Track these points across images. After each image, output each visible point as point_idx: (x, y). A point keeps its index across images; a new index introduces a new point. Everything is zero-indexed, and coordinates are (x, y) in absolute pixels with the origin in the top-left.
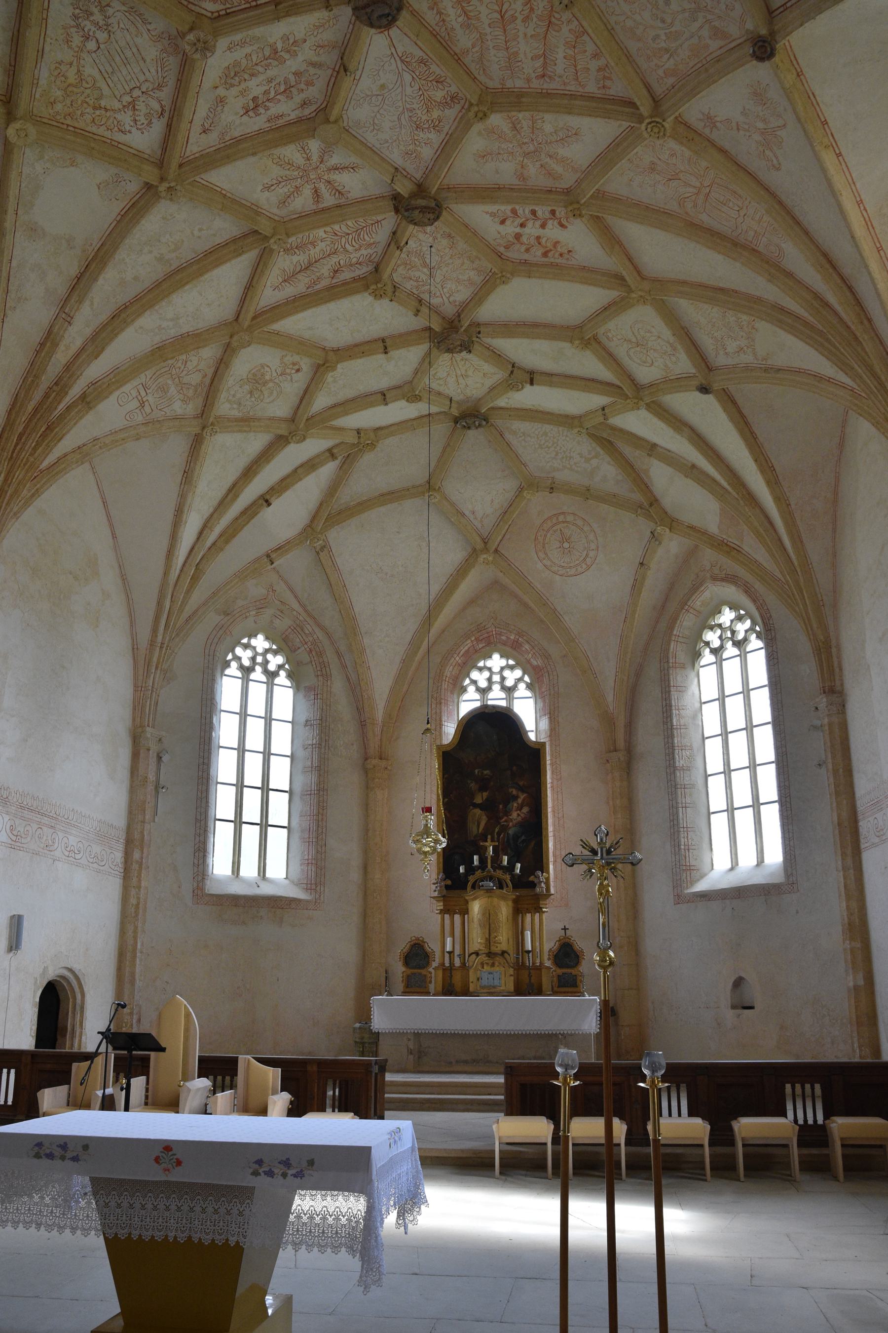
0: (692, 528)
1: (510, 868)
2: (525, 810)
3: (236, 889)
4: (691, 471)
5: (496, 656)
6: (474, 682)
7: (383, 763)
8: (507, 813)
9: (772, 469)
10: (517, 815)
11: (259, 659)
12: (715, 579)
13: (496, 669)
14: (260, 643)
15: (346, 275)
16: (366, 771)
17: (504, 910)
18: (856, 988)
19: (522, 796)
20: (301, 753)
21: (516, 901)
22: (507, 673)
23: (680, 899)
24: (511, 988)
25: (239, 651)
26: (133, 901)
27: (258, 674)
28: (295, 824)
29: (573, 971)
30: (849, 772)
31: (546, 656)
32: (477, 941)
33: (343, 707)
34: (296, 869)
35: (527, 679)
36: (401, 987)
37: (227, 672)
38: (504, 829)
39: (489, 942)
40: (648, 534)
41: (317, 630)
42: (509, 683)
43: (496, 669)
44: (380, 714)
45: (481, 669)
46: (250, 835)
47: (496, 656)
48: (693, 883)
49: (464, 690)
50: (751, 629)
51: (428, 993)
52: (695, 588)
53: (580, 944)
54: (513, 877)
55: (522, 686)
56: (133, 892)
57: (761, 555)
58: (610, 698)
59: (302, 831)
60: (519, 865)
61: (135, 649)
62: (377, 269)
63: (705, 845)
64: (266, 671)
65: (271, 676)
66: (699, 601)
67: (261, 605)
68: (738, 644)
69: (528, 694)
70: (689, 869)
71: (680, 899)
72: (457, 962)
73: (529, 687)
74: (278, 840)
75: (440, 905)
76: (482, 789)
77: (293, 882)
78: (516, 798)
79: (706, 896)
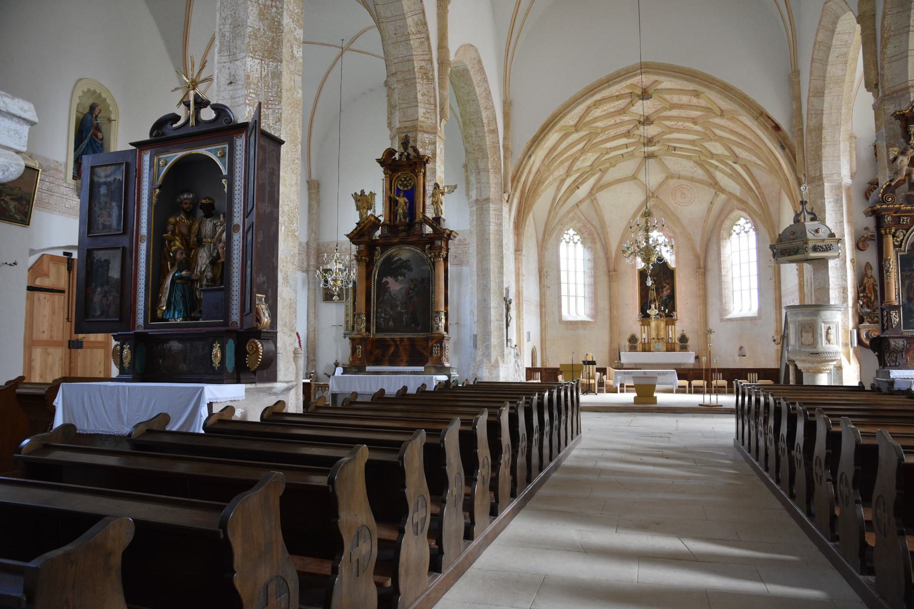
0: (730, 193)
1: (664, 311)
2: (669, 291)
3: (570, 319)
4: (730, 176)
7: (616, 273)
8: (662, 292)
9: (758, 183)
10: (666, 293)
11: (571, 238)
12: (738, 209)
14: (571, 232)
15: (619, 133)
16: (609, 276)
17: (663, 325)
18: (777, 350)
19: (668, 286)
20: (587, 271)
21: (666, 322)
24: (665, 349)
26: (544, 325)
27: (571, 243)
28: (587, 295)
29: (686, 344)
30: (780, 282)
31: (674, 233)
32: (653, 334)
33: (601, 254)
34: (588, 311)
36: (628, 349)
38: (661, 297)
39: (657, 335)
40: (714, 193)
44: (613, 255)
46: (572, 299)
48: (727, 315)
50: (751, 228)
51: (637, 351)
52: (731, 211)
53: (688, 335)
54: (665, 314)
56: (544, 322)
57: (754, 206)
58: (698, 249)
60: (667, 310)
61: (537, 242)
62: (629, 132)
63: (731, 302)
64: (574, 242)
66: (732, 216)
67: (572, 219)
70: (726, 310)
71: (722, 320)
72: (646, 342)
74: (581, 301)
75: (641, 323)
78: (665, 287)
79: (731, 320)
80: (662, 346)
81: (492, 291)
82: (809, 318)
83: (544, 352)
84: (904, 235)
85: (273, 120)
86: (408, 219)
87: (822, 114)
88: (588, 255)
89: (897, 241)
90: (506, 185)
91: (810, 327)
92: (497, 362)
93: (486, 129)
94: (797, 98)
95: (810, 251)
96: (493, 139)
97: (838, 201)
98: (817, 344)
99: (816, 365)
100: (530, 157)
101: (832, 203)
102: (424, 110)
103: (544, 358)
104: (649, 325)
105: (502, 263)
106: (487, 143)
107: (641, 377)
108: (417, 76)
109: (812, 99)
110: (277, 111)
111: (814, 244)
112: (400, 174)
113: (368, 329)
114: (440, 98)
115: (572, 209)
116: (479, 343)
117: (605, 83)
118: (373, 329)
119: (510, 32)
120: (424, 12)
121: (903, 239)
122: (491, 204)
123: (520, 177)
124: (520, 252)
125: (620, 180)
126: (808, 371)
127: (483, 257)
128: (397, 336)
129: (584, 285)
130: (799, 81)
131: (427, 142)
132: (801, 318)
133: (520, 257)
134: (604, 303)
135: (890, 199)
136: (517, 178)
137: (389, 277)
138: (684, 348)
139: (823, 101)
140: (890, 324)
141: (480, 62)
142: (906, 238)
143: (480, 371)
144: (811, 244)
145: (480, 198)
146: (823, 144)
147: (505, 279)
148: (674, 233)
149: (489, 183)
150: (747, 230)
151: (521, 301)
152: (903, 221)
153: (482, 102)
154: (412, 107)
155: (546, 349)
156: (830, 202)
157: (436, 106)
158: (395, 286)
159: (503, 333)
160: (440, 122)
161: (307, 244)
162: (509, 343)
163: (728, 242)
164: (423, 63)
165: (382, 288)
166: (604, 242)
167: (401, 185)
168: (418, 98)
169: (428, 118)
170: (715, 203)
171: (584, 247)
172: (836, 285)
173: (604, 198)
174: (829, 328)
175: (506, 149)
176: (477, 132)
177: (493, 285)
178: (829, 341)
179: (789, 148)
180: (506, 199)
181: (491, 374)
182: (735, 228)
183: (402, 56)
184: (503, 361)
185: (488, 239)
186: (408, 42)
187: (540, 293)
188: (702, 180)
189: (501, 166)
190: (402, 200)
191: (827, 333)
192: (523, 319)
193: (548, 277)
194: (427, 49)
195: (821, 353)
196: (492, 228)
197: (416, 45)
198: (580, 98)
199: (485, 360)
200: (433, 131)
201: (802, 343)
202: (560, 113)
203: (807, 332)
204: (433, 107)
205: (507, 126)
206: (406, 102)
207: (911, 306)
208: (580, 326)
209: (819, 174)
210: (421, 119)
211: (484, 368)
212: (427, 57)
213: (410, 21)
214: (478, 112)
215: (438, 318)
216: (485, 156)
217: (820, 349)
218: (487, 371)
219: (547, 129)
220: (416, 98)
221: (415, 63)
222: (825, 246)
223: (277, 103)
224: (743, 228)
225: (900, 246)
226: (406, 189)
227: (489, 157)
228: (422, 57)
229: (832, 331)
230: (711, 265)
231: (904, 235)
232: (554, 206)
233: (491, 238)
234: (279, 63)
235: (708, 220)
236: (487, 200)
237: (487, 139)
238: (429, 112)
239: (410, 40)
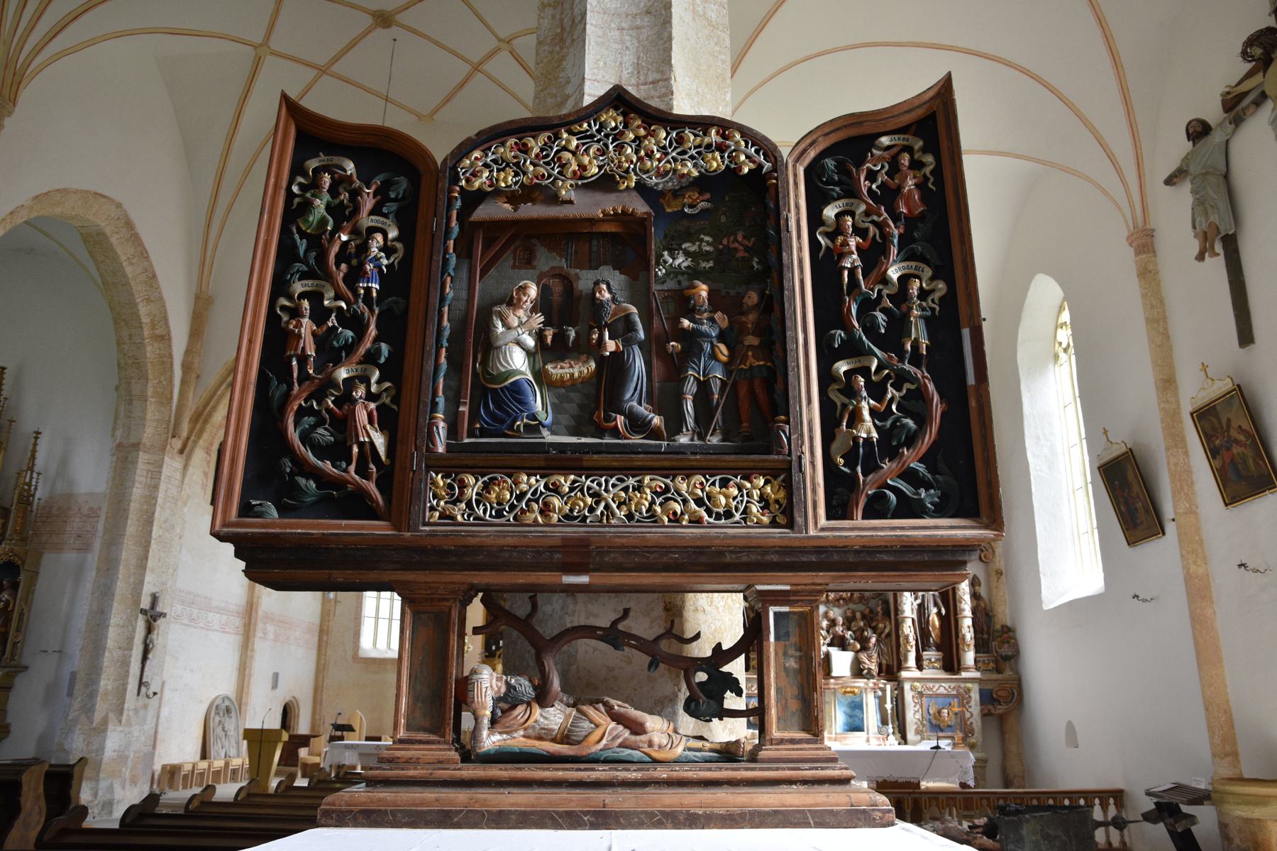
81: (117, 598)
83: (318, 707)
92: (105, 722)
93: (146, 333)
105: (148, 551)
116: (78, 687)
122: (141, 453)
123: (210, 415)
136: (203, 417)
141: (129, 225)
143: (69, 739)
147: (148, 578)
149: (143, 419)
151: (253, 621)
153: (139, 290)
175: (186, 367)
177: (122, 587)
184: (120, 721)
185: (126, 510)
192: (253, 651)
196: (138, 491)
199: (83, 718)
211: (77, 732)
216: (144, 377)
218: (81, 738)
227: (150, 377)
236: (136, 446)
237: (149, 348)
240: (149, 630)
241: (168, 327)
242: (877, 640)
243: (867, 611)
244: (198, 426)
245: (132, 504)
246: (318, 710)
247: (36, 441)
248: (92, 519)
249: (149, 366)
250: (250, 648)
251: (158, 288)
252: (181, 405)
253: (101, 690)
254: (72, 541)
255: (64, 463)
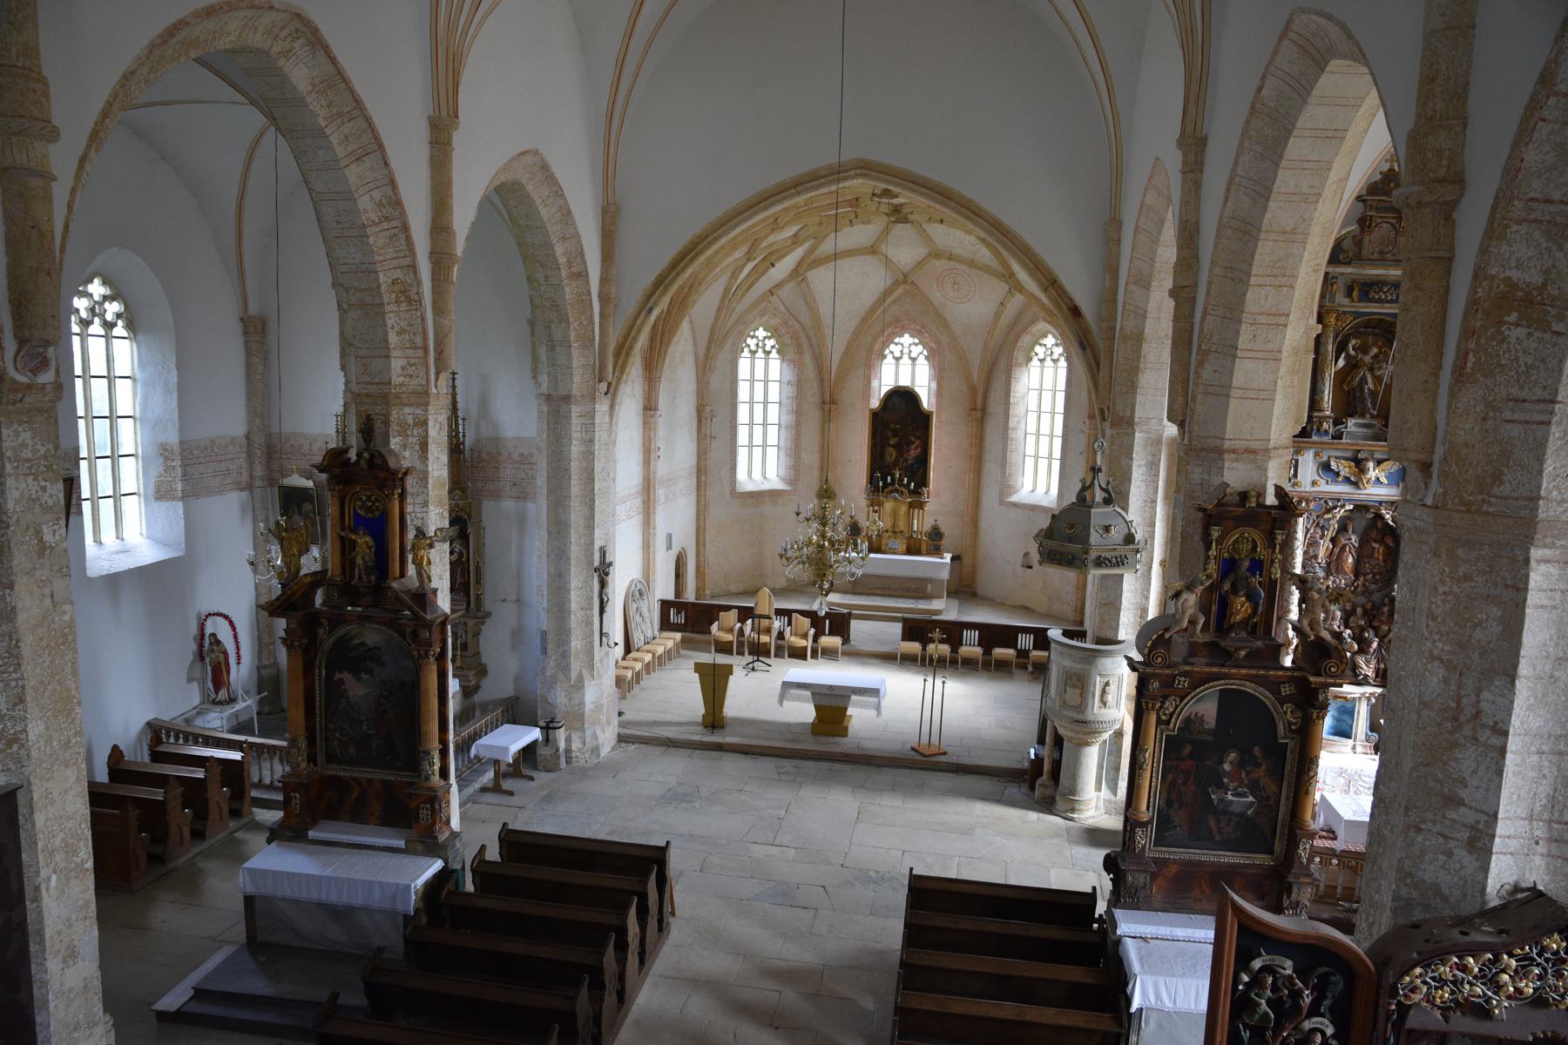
1: (909, 484)
2: (919, 450)
3: (750, 487)
5: (907, 336)
6: (892, 353)
8: (908, 451)
10: (914, 452)
12: (1045, 320)
13: (906, 345)
14: (761, 333)
19: (918, 442)
20: (785, 401)
22: (913, 347)
23: (1002, 503)
24: (904, 549)
25: (749, 341)
26: (703, 503)
28: (781, 444)
29: (938, 543)
33: (811, 373)
34: (783, 472)
35: (925, 352)
37: (743, 355)
38: (906, 460)
41: (796, 323)
42: (914, 355)
43: (906, 345)
45: (896, 344)
46: (757, 452)
47: (907, 336)
48: (1010, 495)
49: (885, 357)
52: (1033, 321)
53: (944, 529)
55: (922, 357)
56: (703, 498)
58: (975, 376)
59: (787, 449)
61: (697, 359)
64: (765, 351)
65: (767, 353)
68: (1055, 361)
69: (926, 362)
70: (1009, 487)
73: (927, 358)
74: (772, 453)
76: (895, 435)
77: (780, 478)
78: (913, 443)
79: (1015, 505)
80: (901, 544)
81: (573, 562)
82: (1079, 666)
84: (1177, 707)
85: (7, 702)
86: (373, 577)
87: (1145, 317)
88: (789, 375)
89: (1165, 714)
90: (602, 367)
91: (1079, 680)
92: (581, 678)
93: (564, 273)
94: (1112, 269)
95: (1090, 565)
96: (578, 287)
97: (1153, 465)
98: (1086, 707)
99: (1081, 736)
100: (650, 311)
101: (1144, 468)
102: (403, 362)
103: (702, 559)
104: (880, 504)
105: (593, 510)
106: (567, 297)
107: (829, 695)
108: (386, 300)
109: (1132, 287)
110: (13, 684)
111: (1099, 554)
112: (358, 489)
113: (311, 759)
114: (436, 333)
115: (763, 298)
116: (550, 646)
117: (790, 188)
118: (321, 758)
119: (615, 83)
120: (392, 182)
121: (1174, 712)
122: (573, 407)
124: (652, 412)
125: (848, 251)
126: (1070, 741)
127: (558, 501)
128: (363, 774)
129: (779, 425)
130: (1119, 240)
131: (411, 422)
132: (1067, 663)
133: (652, 420)
134: (811, 458)
135: (1160, 660)
136: (624, 351)
137: (346, 673)
138: (936, 551)
139: (1147, 298)
140: (1131, 846)
141: (545, 167)
142: (1177, 711)
144: (1093, 555)
145: (553, 393)
146: (1142, 365)
148: (938, 343)
149: (569, 367)
150: (1055, 356)
151: (652, 498)
152: (1179, 684)
153: (554, 230)
154: (380, 357)
155: (705, 546)
156: (1140, 466)
157: (426, 350)
158: (357, 689)
159: (592, 630)
160: (437, 380)
161: (248, 436)
162: (604, 638)
163: (1024, 369)
164: (398, 274)
165: (334, 690)
166: (817, 352)
167: (361, 508)
168: (390, 340)
169: (411, 376)
170: (1008, 306)
171: (783, 360)
172: (1131, 604)
173: (820, 279)
174: (1107, 684)
175: (604, 299)
176: (546, 277)
177: (575, 551)
178: (1104, 703)
179: (1093, 351)
180: (605, 389)
181: (570, 700)
182: (1038, 349)
183: (355, 261)
185: (567, 470)
186: (364, 239)
187: (698, 448)
188: (989, 267)
189: (593, 333)
190: (364, 541)
191: (1104, 692)
193: (714, 420)
194: (405, 248)
195: (1090, 722)
196: (576, 449)
197: (381, 243)
198: (745, 211)
199: (561, 676)
200: (422, 397)
201: (1064, 701)
202: (708, 236)
203: (1074, 686)
204: (420, 353)
205: (608, 256)
206: (367, 346)
207: (1171, 812)
208: (766, 499)
209: (1128, 414)
210: (396, 380)
211: (559, 689)
212: (406, 262)
213: (364, 203)
214: (549, 247)
215: (427, 762)
216: (564, 320)
217: (1090, 717)
218: (563, 694)
219: (682, 264)
220: (386, 341)
221: (381, 276)
222: (1116, 558)
223: (11, 669)
224: (1049, 353)
225: (1168, 722)
226: (370, 515)
227: (571, 320)
228: (395, 263)
229: (1112, 689)
230: (994, 406)
231: (1177, 707)
232: (726, 299)
233: (573, 468)
234: (8, 591)
235: (994, 330)
236: (567, 399)
237: (567, 289)
238: (414, 364)
239: (368, 237)
240: (603, 584)
241: (584, 262)
242: (1379, 644)
243: (1369, 606)
244: (620, 362)
245: (572, 463)
246: (702, 554)
247: (454, 383)
248: (523, 467)
249: (569, 309)
250: (651, 526)
251: (574, 223)
252: (603, 344)
253: (572, 650)
254: (508, 488)
255: (484, 404)
